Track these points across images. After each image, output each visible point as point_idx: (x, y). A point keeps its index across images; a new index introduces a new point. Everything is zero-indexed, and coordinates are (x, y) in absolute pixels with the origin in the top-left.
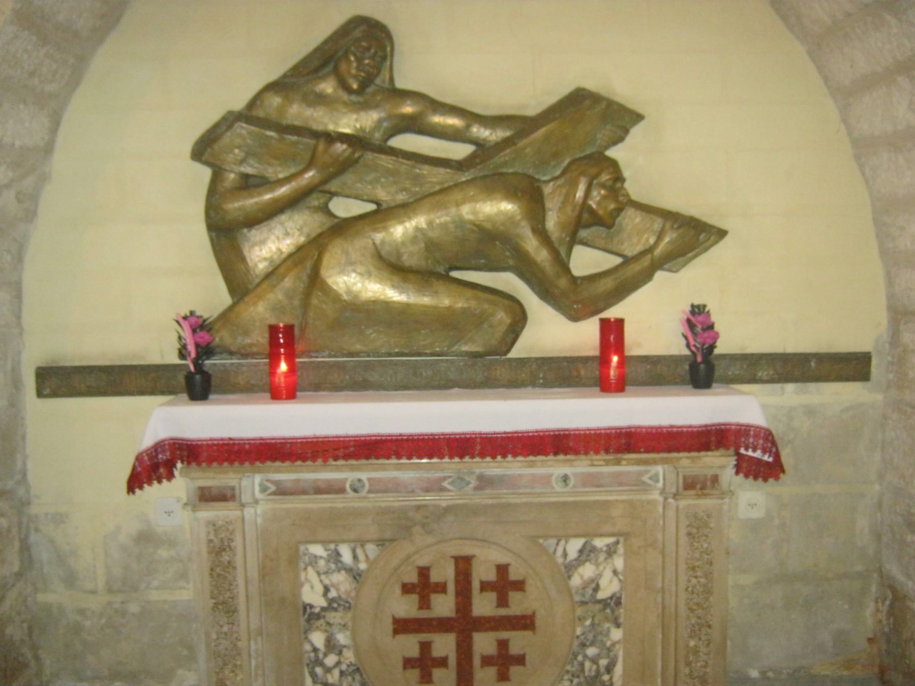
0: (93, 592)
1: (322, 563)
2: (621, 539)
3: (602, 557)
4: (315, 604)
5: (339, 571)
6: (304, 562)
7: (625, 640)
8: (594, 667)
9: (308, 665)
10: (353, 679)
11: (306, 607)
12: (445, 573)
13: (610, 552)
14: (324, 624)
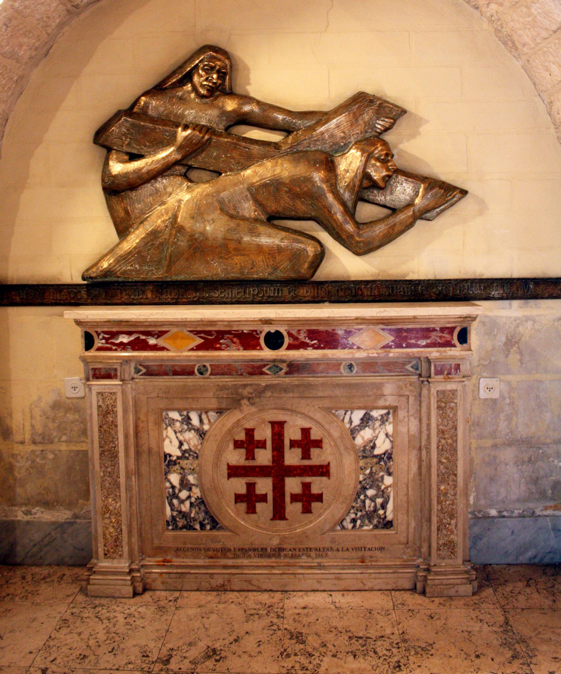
1: (178, 424)
2: (391, 411)
3: (377, 424)
4: (173, 454)
5: (190, 431)
6: (166, 424)
7: (395, 485)
8: (373, 504)
9: (168, 498)
10: (200, 509)
11: (166, 455)
13: (383, 420)
14: (179, 468)
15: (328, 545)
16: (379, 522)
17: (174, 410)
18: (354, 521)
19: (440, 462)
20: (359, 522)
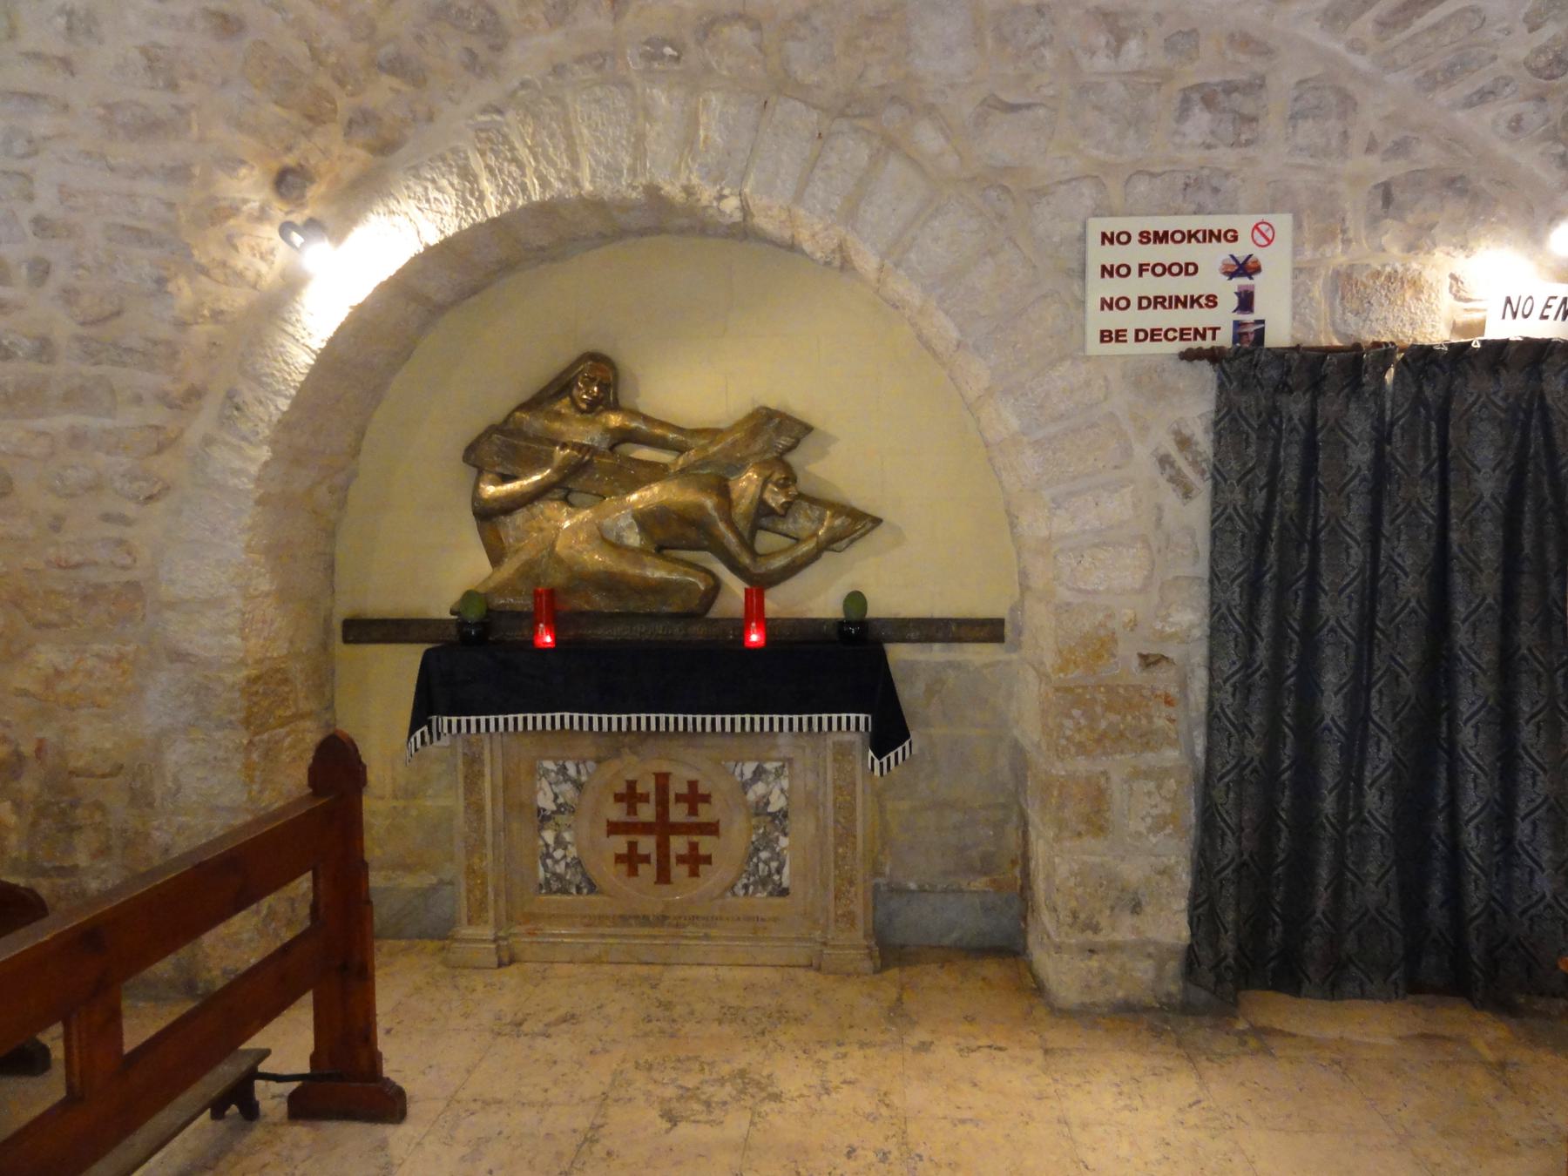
0: (382, 798)
2: (787, 764)
3: (771, 778)
4: (547, 807)
7: (791, 847)
11: (540, 810)
12: (648, 786)
13: (778, 774)
15: (717, 913)
16: (773, 889)
17: (548, 758)
18: (746, 887)
19: (836, 822)
20: (751, 888)
